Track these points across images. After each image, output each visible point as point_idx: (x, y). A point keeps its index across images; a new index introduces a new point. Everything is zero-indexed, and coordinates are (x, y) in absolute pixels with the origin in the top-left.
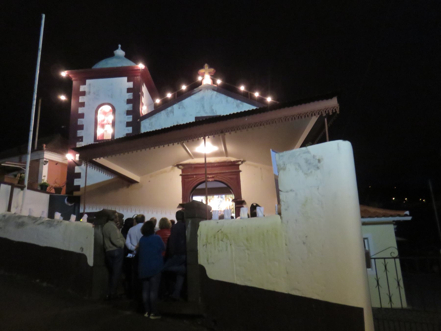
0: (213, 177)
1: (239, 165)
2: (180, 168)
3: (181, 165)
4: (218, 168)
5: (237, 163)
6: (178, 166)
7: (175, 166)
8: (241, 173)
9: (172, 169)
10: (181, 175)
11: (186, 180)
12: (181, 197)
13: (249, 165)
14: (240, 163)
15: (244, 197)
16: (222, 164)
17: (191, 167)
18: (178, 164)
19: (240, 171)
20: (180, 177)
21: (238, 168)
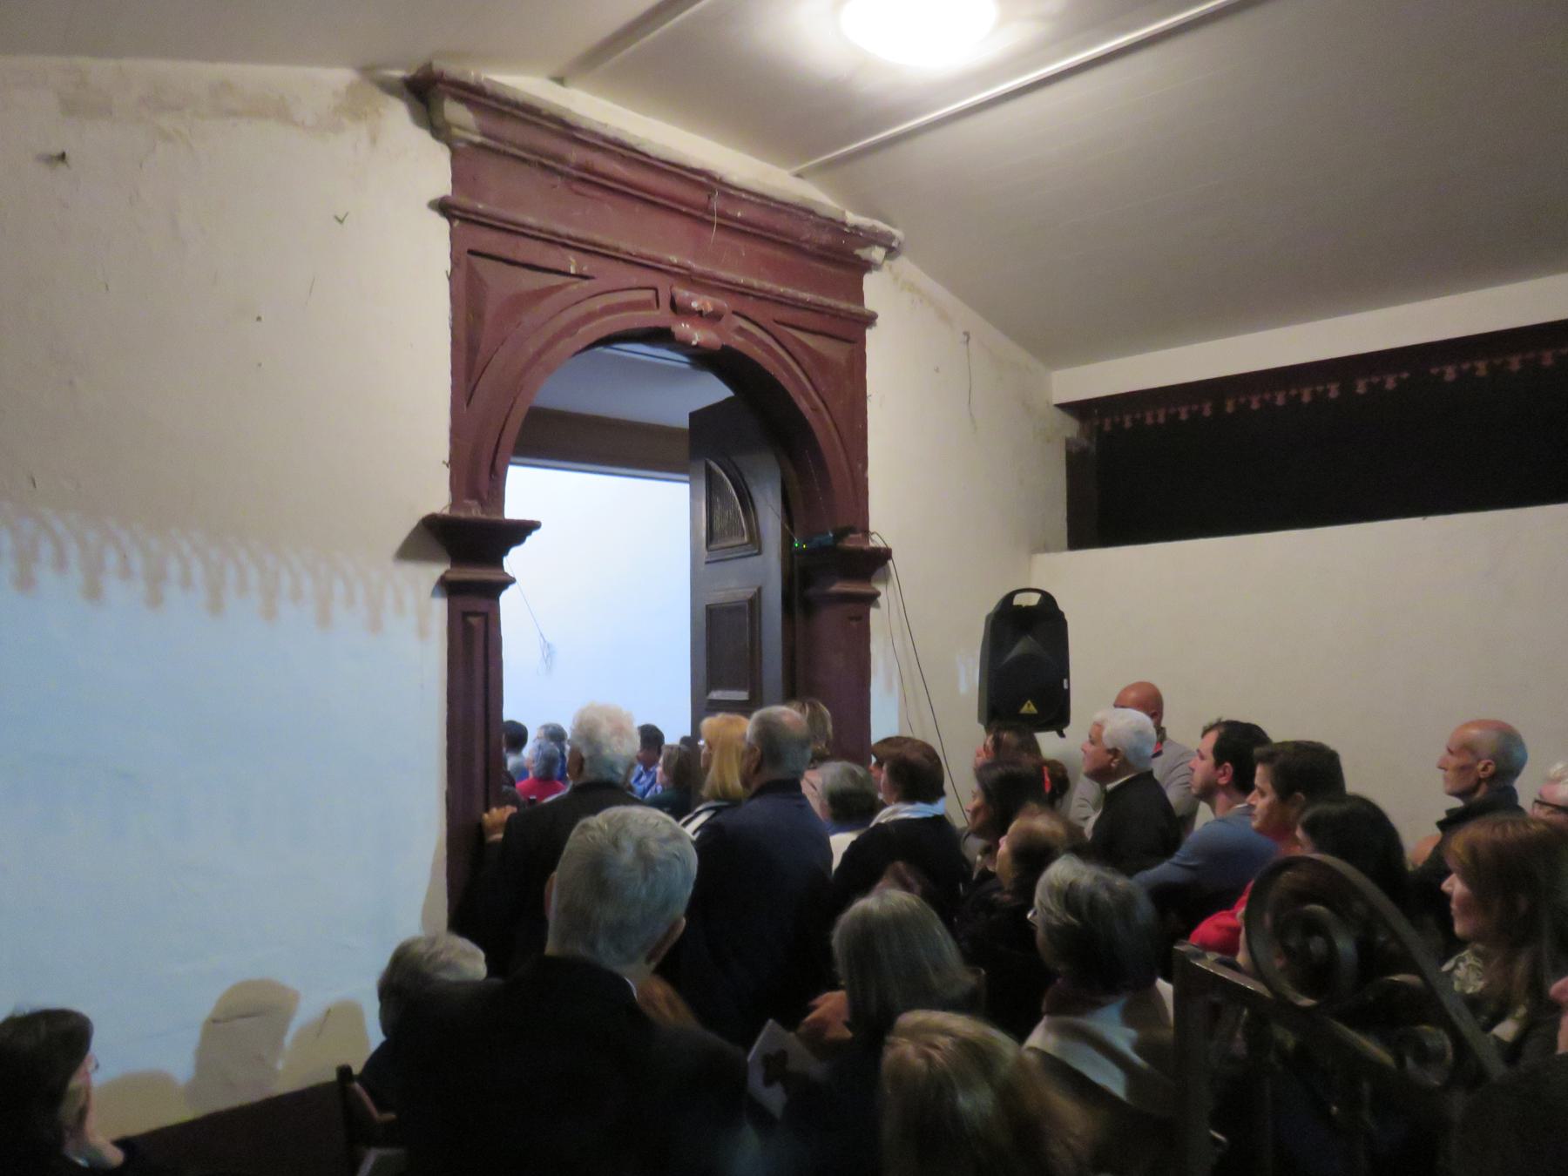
0: (715, 317)
1: (867, 266)
2: (439, 130)
3: (473, 95)
4: (743, 246)
5: (863, 253)
6: (425, 93)
7: (388, 87)
8: (870, 334)
9: (352, 108)
10: (443, 207)
11: (502, 282)
12: (443, 449)
13: (912, 288)
14: (877, 253)
15: (886, 519)
16: (782, 223)
17: (547, 165)
18: (453, 69)
19: (869, 320)
20: (440, 227)
21: (859, 298)
